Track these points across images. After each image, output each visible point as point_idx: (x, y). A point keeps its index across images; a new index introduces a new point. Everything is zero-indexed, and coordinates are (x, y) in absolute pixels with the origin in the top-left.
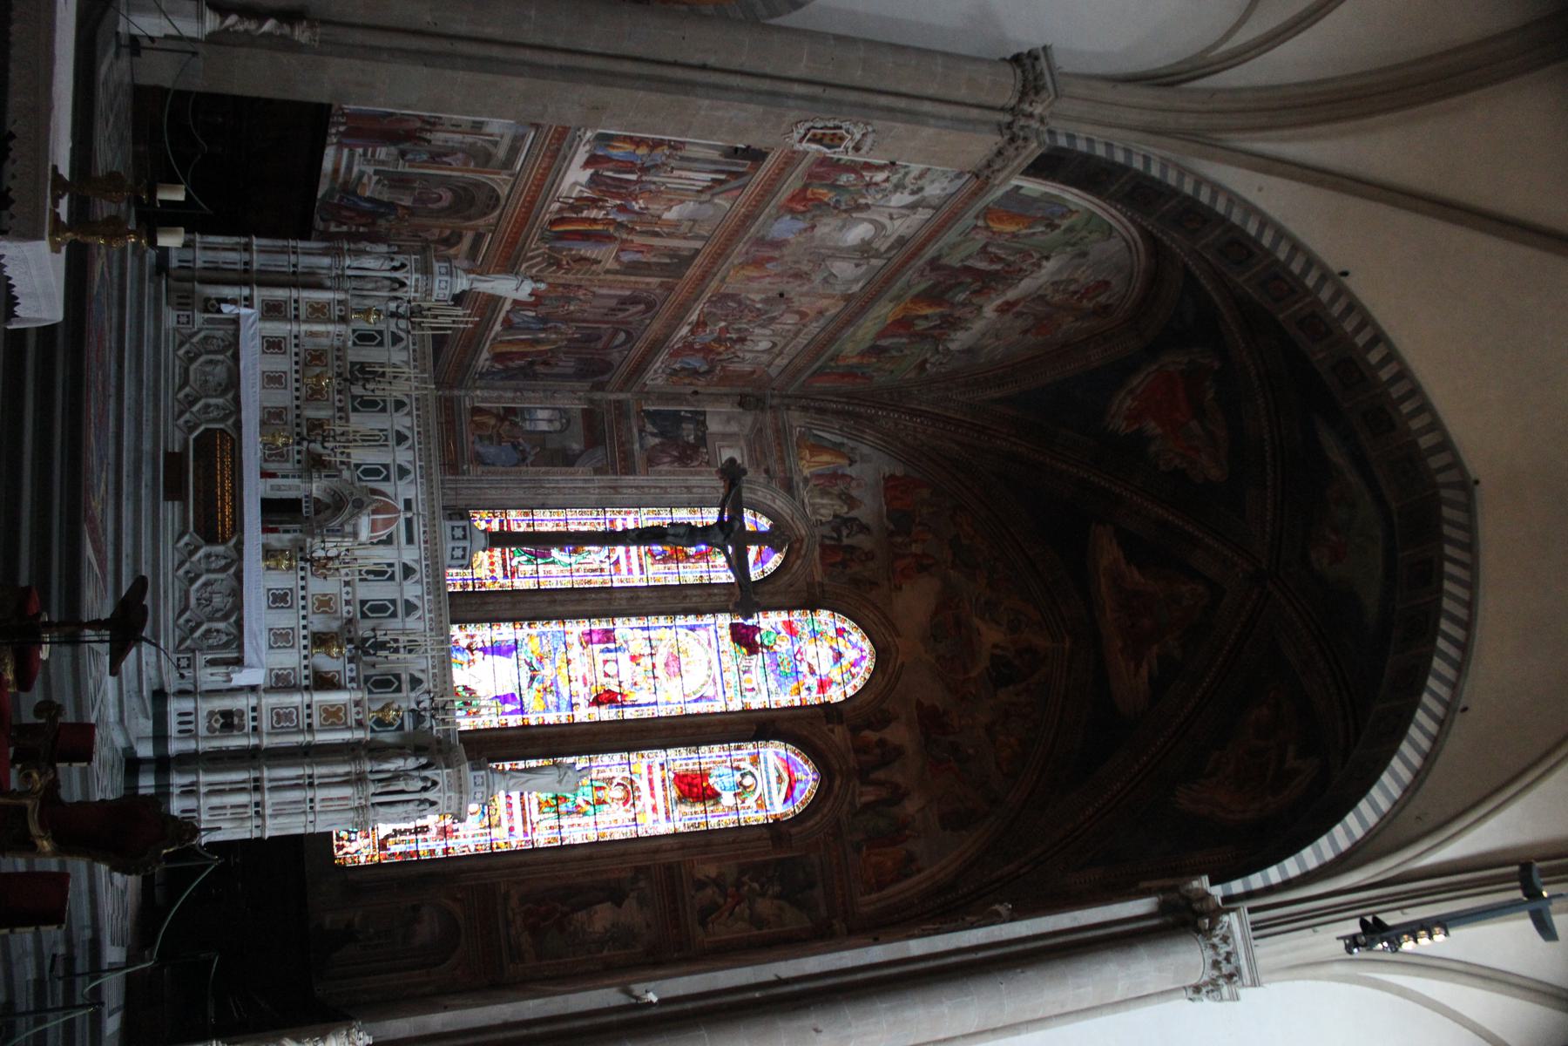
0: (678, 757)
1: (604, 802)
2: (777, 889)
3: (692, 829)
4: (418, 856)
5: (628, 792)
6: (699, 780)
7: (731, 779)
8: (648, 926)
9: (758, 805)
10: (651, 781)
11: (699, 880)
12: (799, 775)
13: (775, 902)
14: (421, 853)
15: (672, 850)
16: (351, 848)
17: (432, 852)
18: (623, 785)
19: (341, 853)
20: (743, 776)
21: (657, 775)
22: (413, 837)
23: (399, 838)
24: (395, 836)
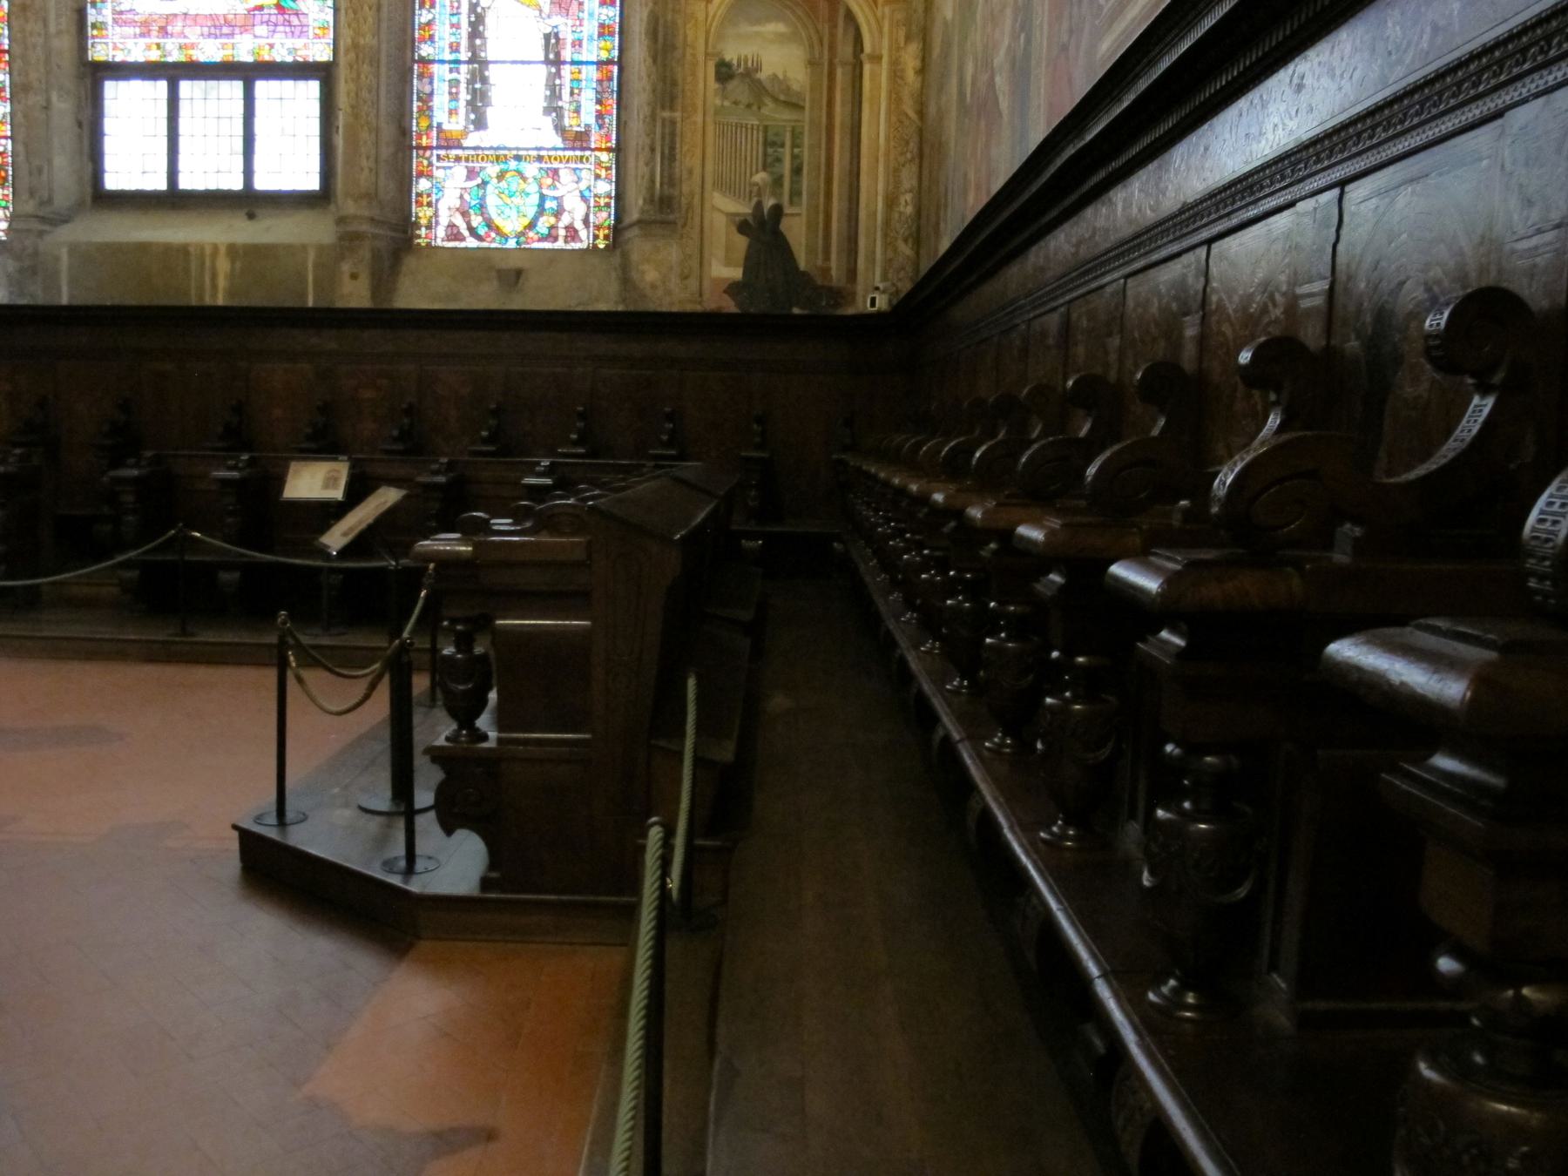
4: (609, 62)
14: (604, 56)
16: (575, 211)
19: (583, 234)
22: (566, 70)
23: (565, 101)
24: (559, 111)
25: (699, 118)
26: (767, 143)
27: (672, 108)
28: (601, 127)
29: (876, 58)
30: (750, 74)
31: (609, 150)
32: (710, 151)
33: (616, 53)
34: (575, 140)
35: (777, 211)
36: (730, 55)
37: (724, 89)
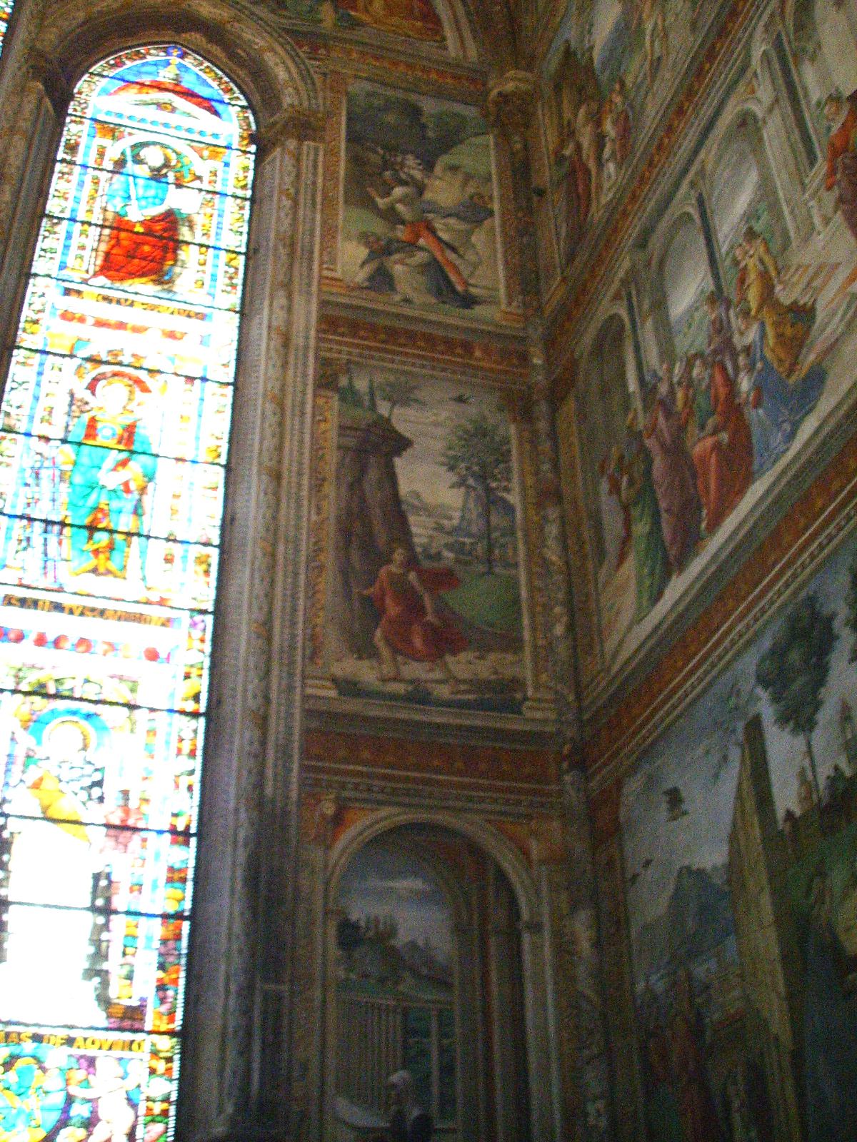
0: (58, 257)
1: (130, 430)
2: (411, 161)
3: (239, 280)
4: (179, 916)
5: (115, 374)
6: (123, 235)
7: (141, 182)
8: (460, 400)
9: (214, 156)
10: (100, 324)
11: (371, 278)
12: (166, 75)
13: (438, 169)
14: (172, 908)
15: (289, 310)
17: (175, 876)
18: (95, 380)
20: (138, 160)
21: (88, 305)
23: (113, 965)
24: (104, 975)
25: (318, 994)
26: (409, 1032)
27: (278, 981)
28: (163, 1000)
29: (536, 928)
30: (382, 937)
31: (171, 1033)
32: (332, 1041)
33: (187, 905)
34: (122, 1019)
35: (424, 1122)
36: (358, 913)
37: (350, 957)
